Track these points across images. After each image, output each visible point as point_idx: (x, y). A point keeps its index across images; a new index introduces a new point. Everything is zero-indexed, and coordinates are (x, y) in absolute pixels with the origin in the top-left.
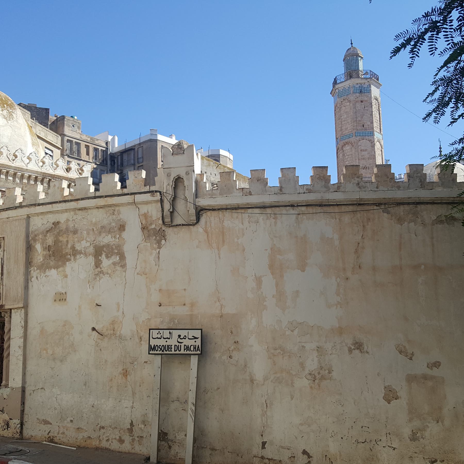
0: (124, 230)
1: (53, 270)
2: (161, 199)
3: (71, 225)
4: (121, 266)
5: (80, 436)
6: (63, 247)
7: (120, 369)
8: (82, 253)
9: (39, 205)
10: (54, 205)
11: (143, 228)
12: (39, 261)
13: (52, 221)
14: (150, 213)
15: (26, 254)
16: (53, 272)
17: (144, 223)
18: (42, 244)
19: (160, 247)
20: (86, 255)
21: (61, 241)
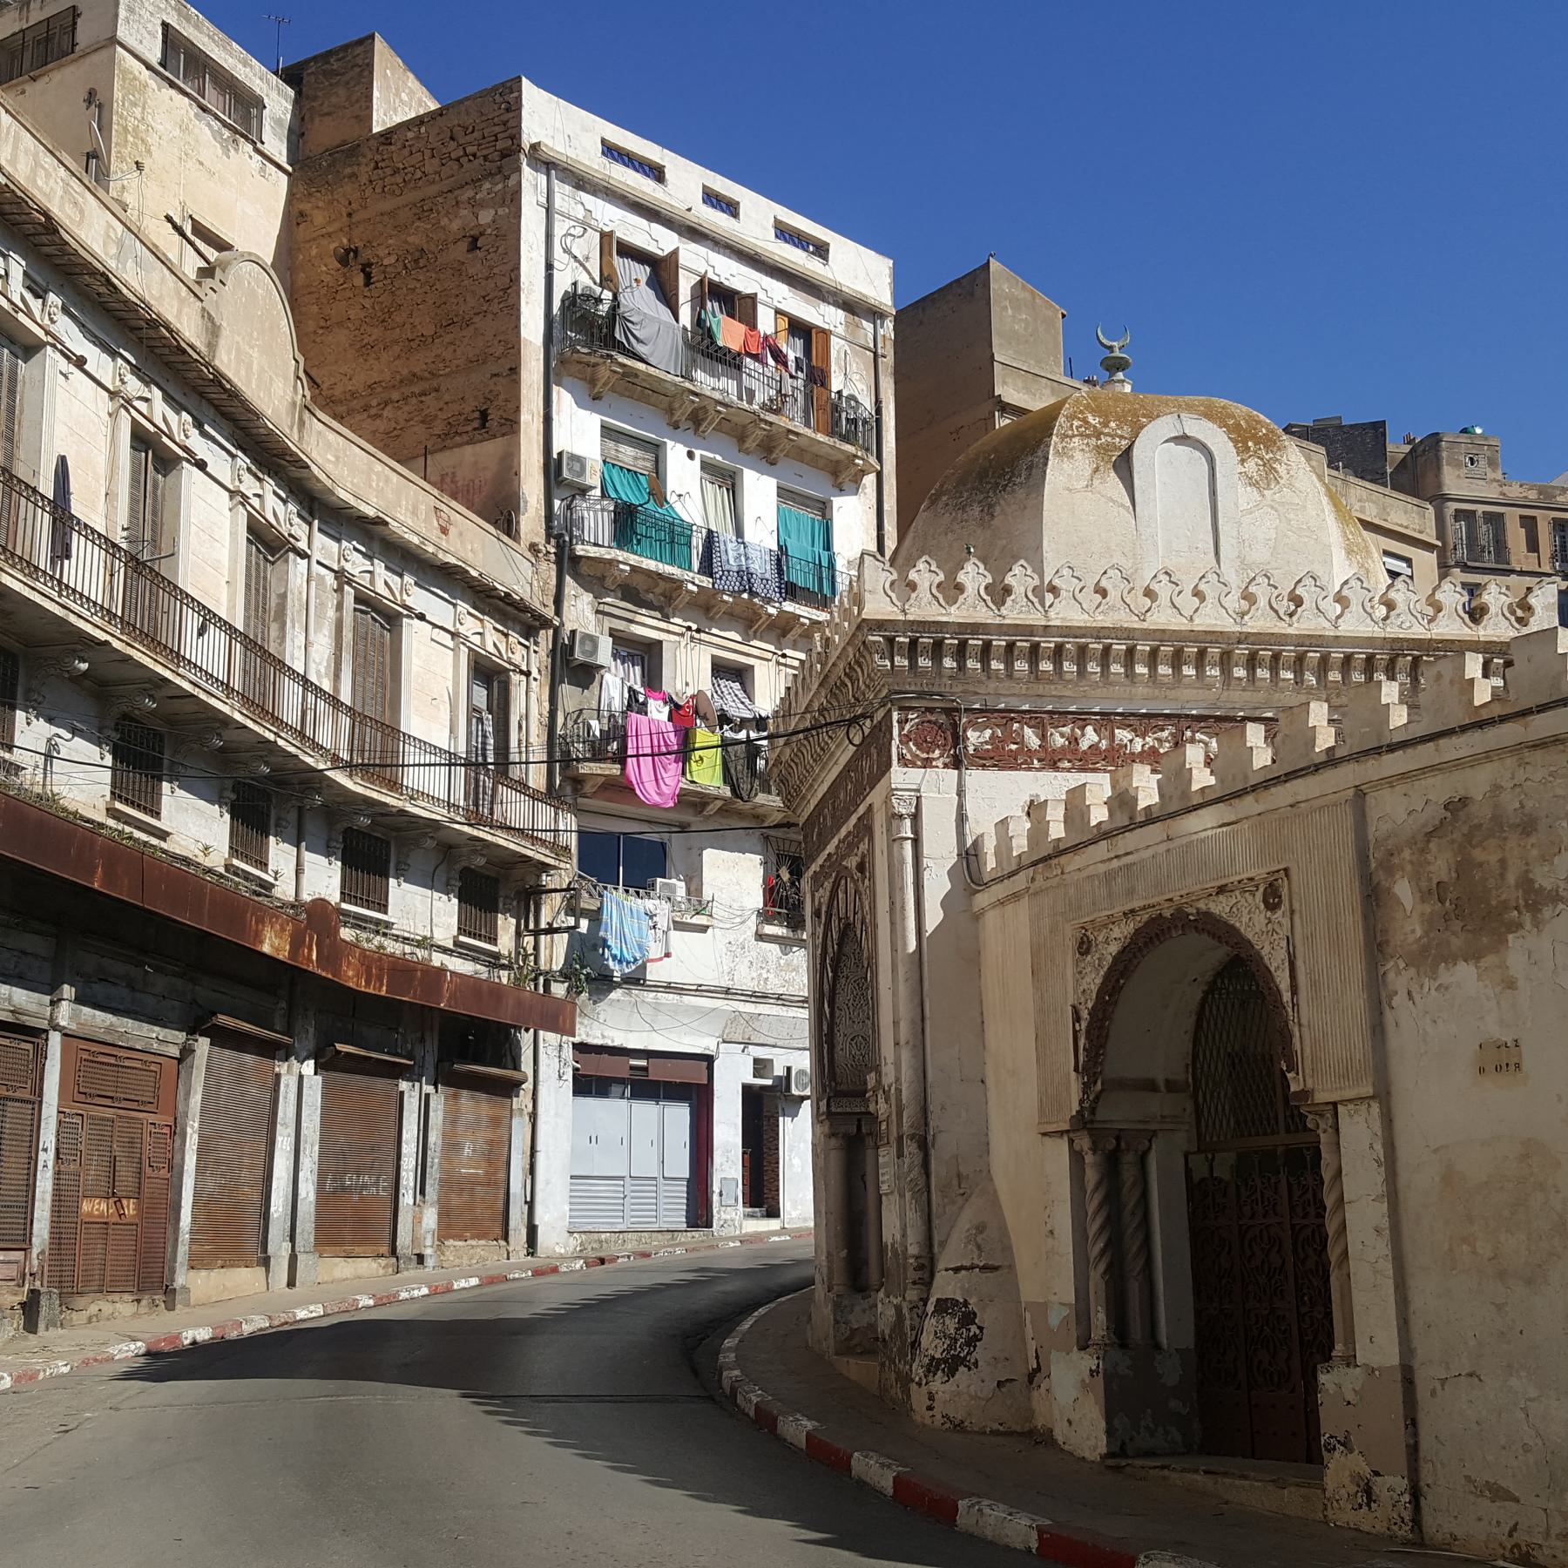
1: (1462, 966)
3: (1510, 802)
6: (1491, 883)
9: (1392, 748)
10: (1442, 742)
12: (1411, 939)
13: (1443, 799)
15: (1365, 917)
18: (1415, 879)
21: (1481, 865)
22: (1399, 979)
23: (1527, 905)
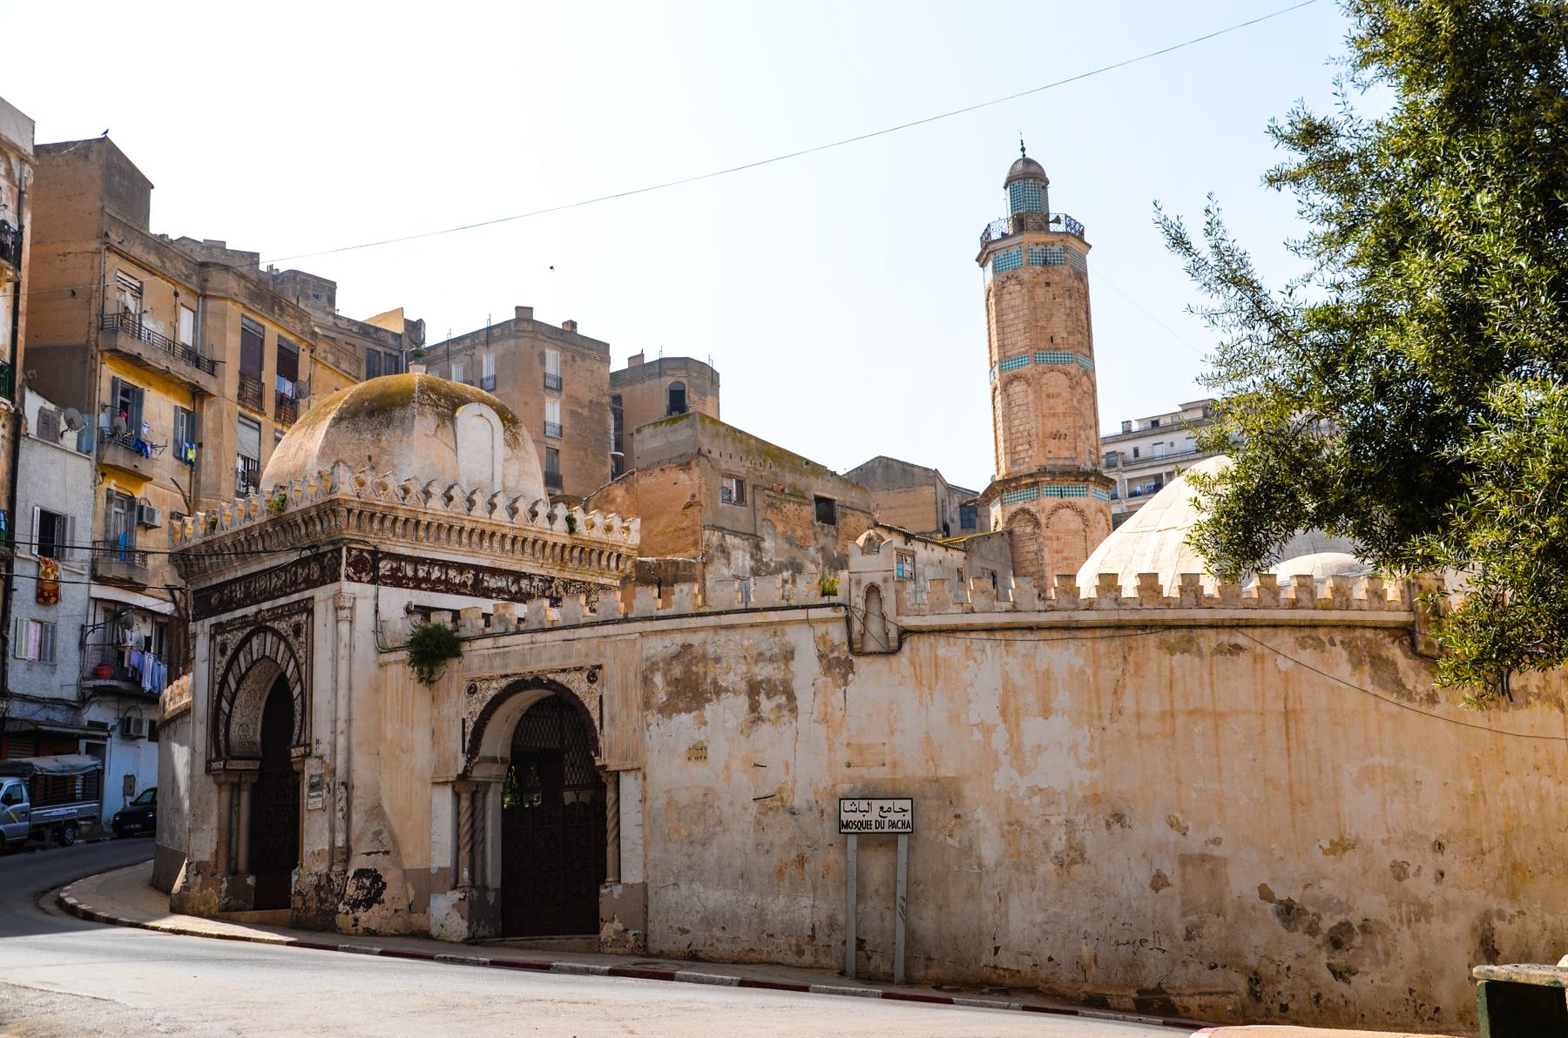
3: (711, 650)
5: (739, 949)
7: (794, 854)
11: (821, 657)
18: (665, 675)
19: (846, 684)
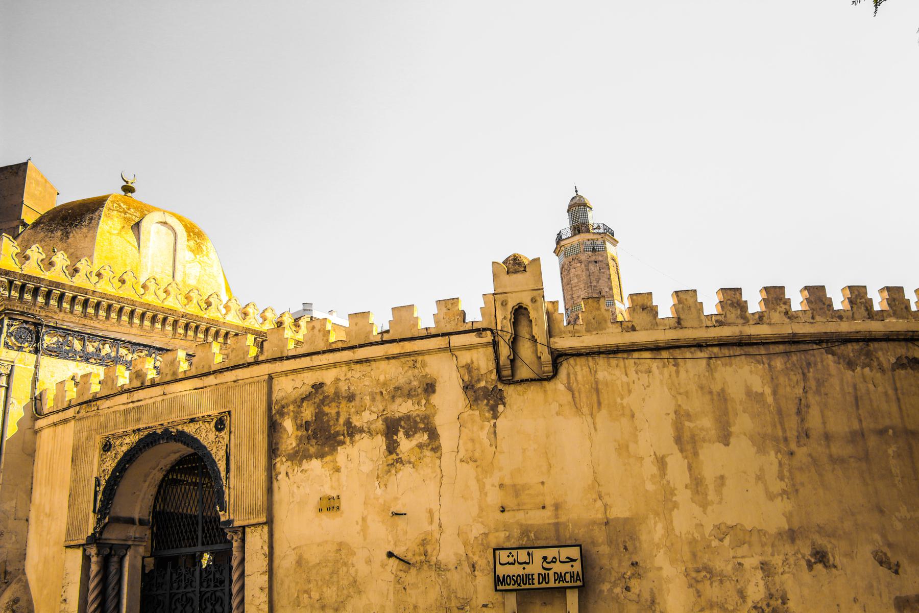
0: (434, 391)
2: (494, 340)
3: (343, 387)
4: (432, 449)
6: (331, 423)
8: (364, 431)
14: (475, 364)
16: (315, 463)
17: (466, 378)
20: (370, 433)
22: (282, 466)
23: (348, 434)
